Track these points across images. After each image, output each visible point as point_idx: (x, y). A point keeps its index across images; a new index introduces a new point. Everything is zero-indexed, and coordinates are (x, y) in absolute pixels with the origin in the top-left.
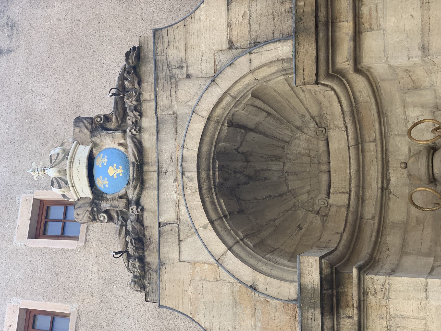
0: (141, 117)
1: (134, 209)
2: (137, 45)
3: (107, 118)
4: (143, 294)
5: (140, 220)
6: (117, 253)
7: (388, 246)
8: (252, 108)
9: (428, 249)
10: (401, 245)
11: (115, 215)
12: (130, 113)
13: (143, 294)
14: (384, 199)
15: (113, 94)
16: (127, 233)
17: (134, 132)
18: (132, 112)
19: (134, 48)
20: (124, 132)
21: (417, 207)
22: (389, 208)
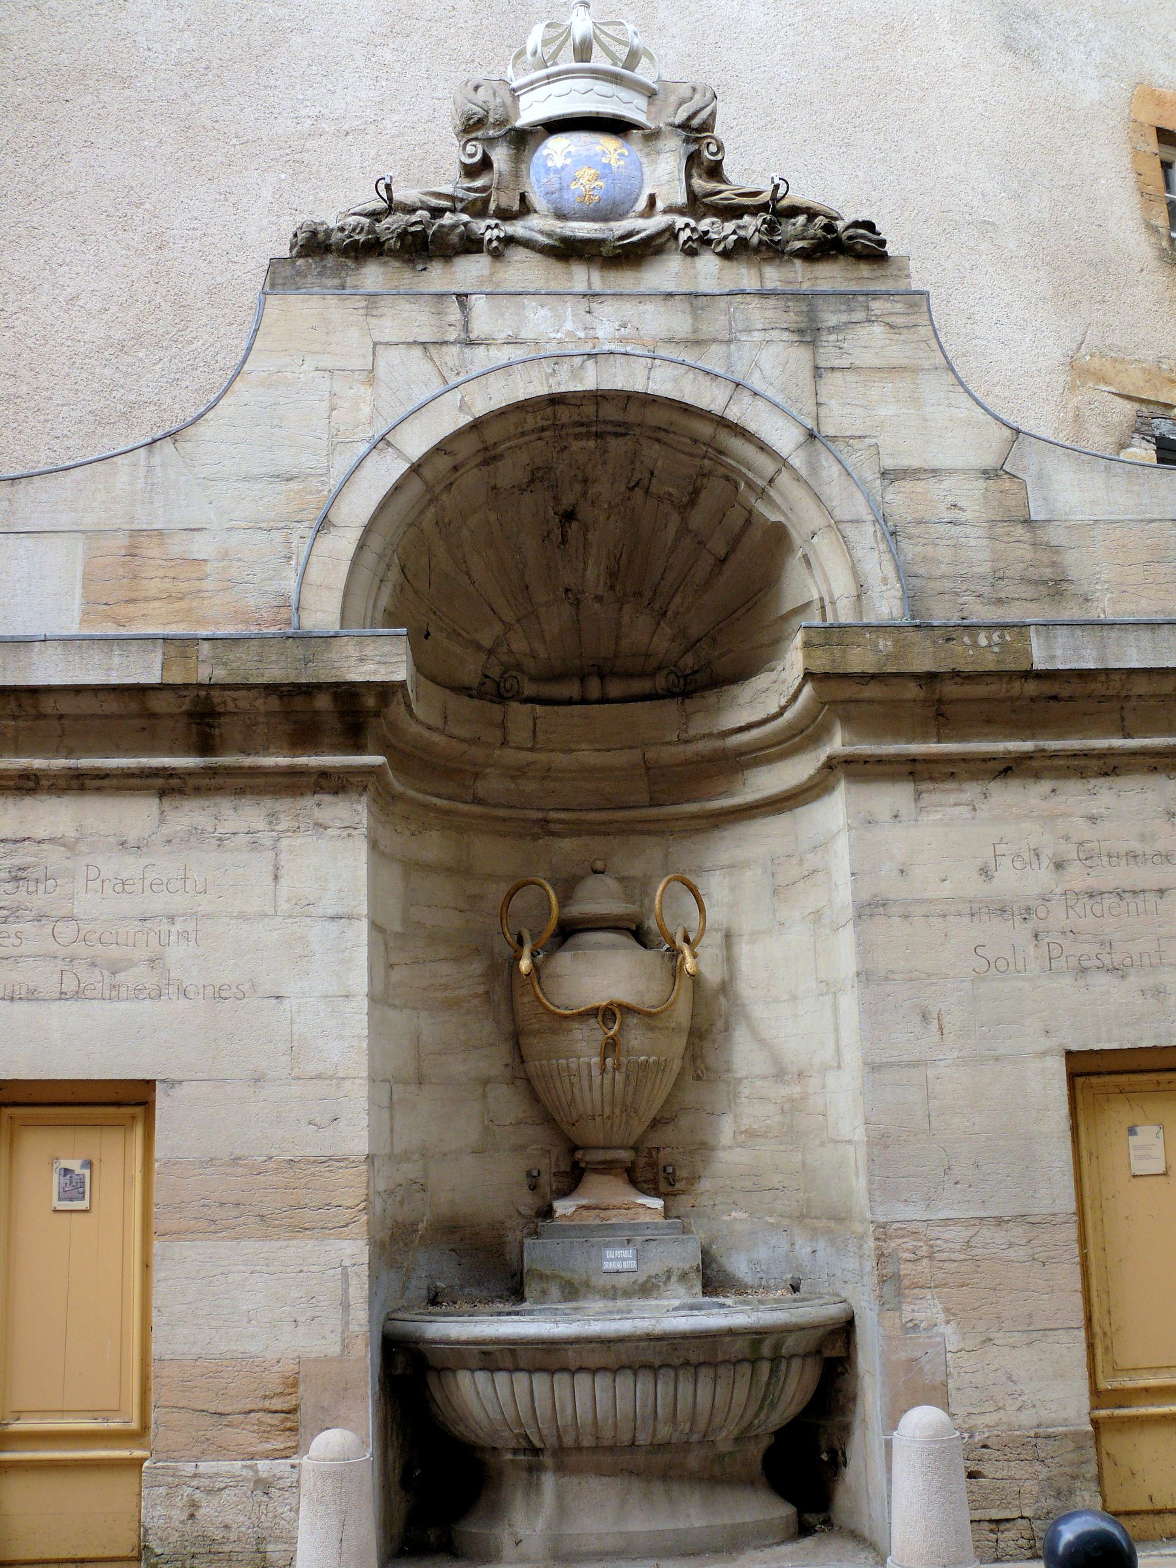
0: (718, 254)
1: (496, 232)
2: (890, 249)
3: (715, 171)
4: (286, 254)
5: (471, 245)
6: (388, 187)
8: (740, 522)
11: (478, 183)
12: (730, 226)
13: (286, 254)
15: (777, 187)
16: (437, 212)
17: (683, 236)
18: (734, 232)
19: (882, 243)
20: (681, 211)
21: (510, 896)
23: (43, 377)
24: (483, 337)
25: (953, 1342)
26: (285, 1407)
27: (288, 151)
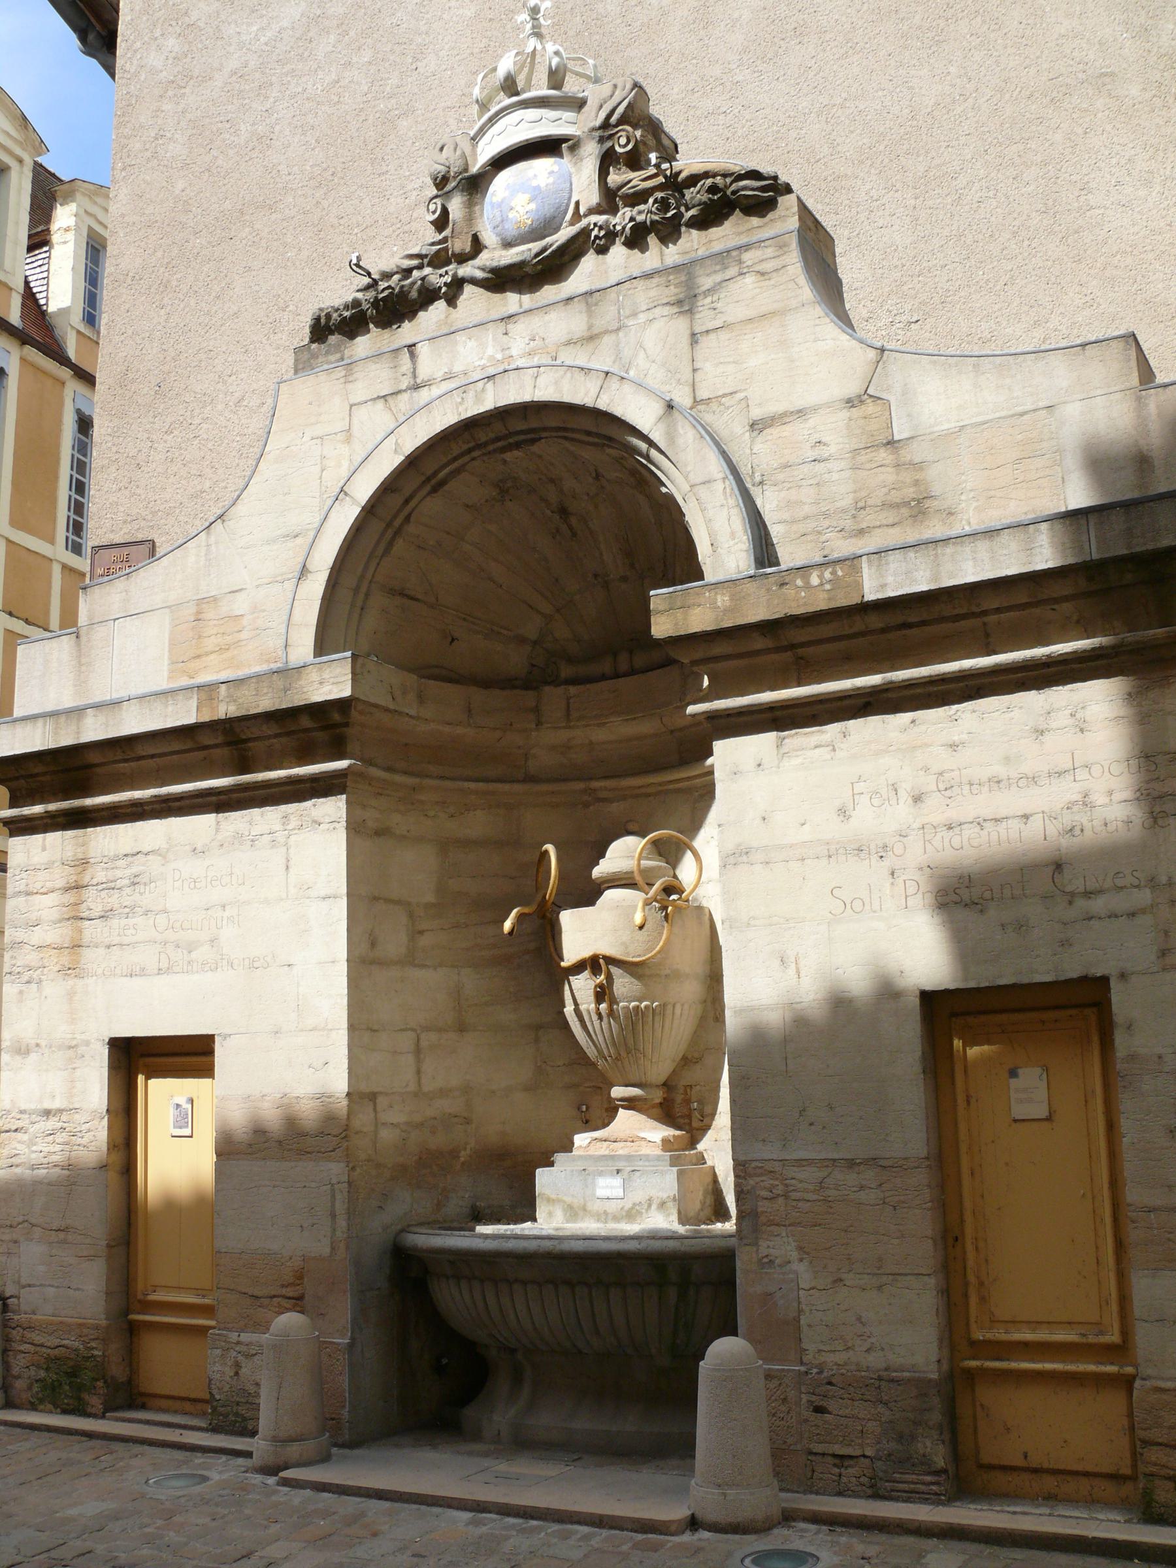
5: (428, 296)
23: (220, 471)
24: (426, 379)
25: (806, 1280)
26: (296, 1295)
27: (398, 226)
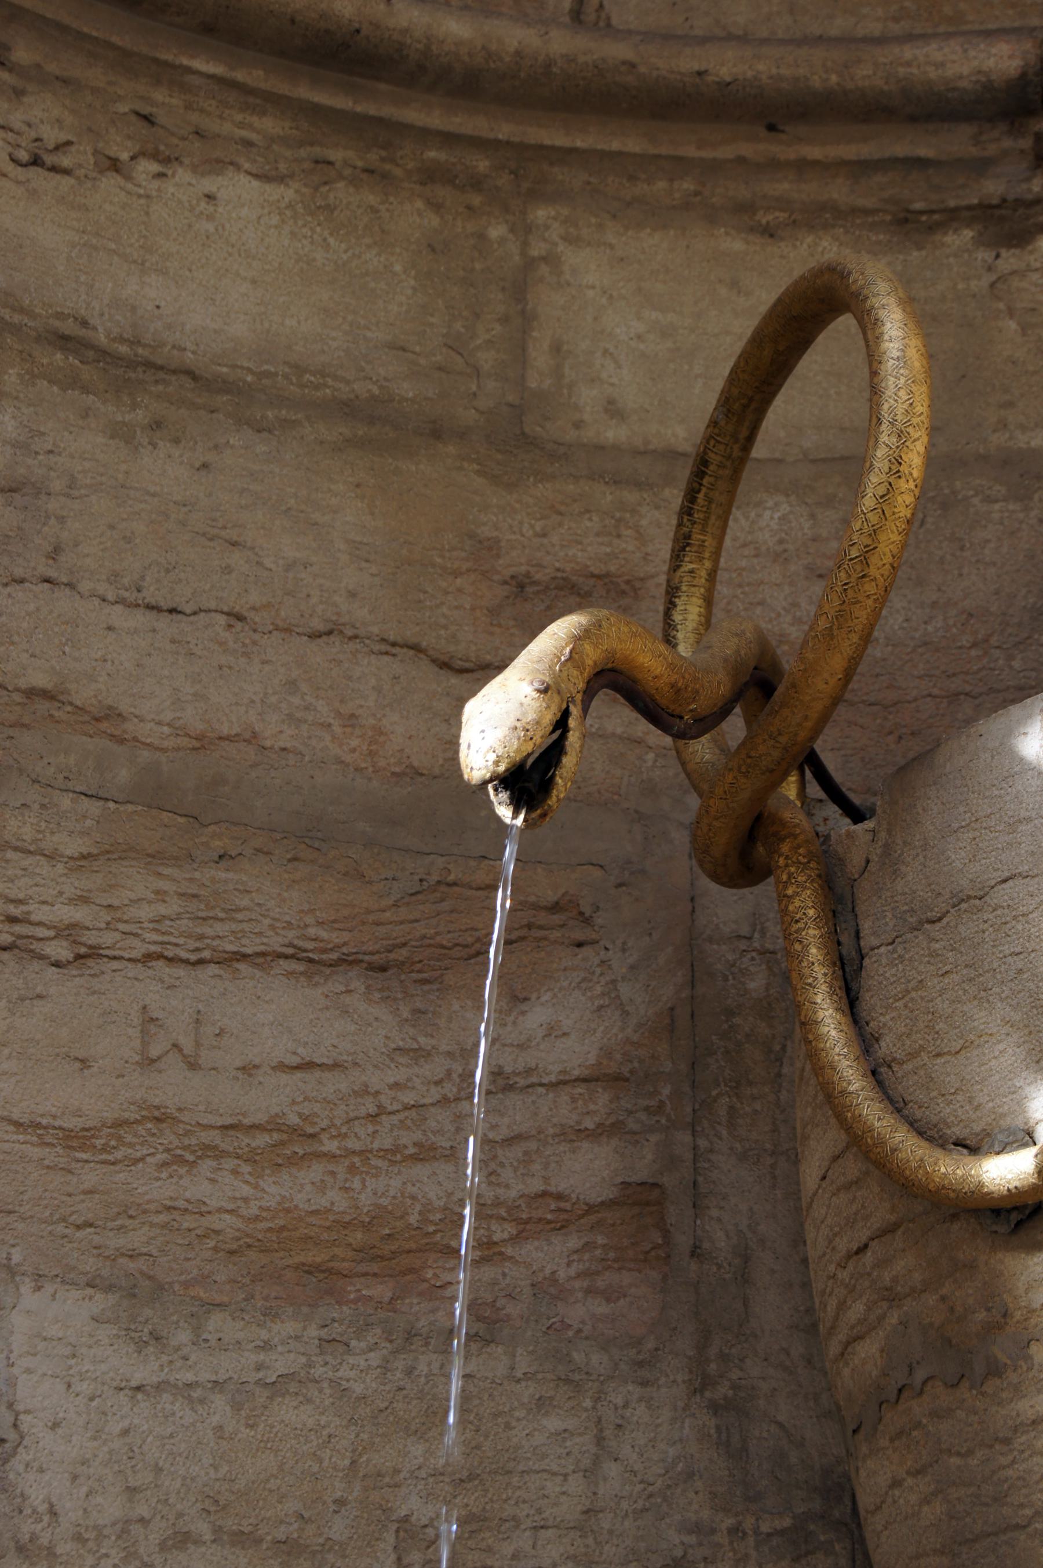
7: (110, 182)
9: (41, 680)
10: (135, 342)
14: (901, 149)
22: (769, 232)
